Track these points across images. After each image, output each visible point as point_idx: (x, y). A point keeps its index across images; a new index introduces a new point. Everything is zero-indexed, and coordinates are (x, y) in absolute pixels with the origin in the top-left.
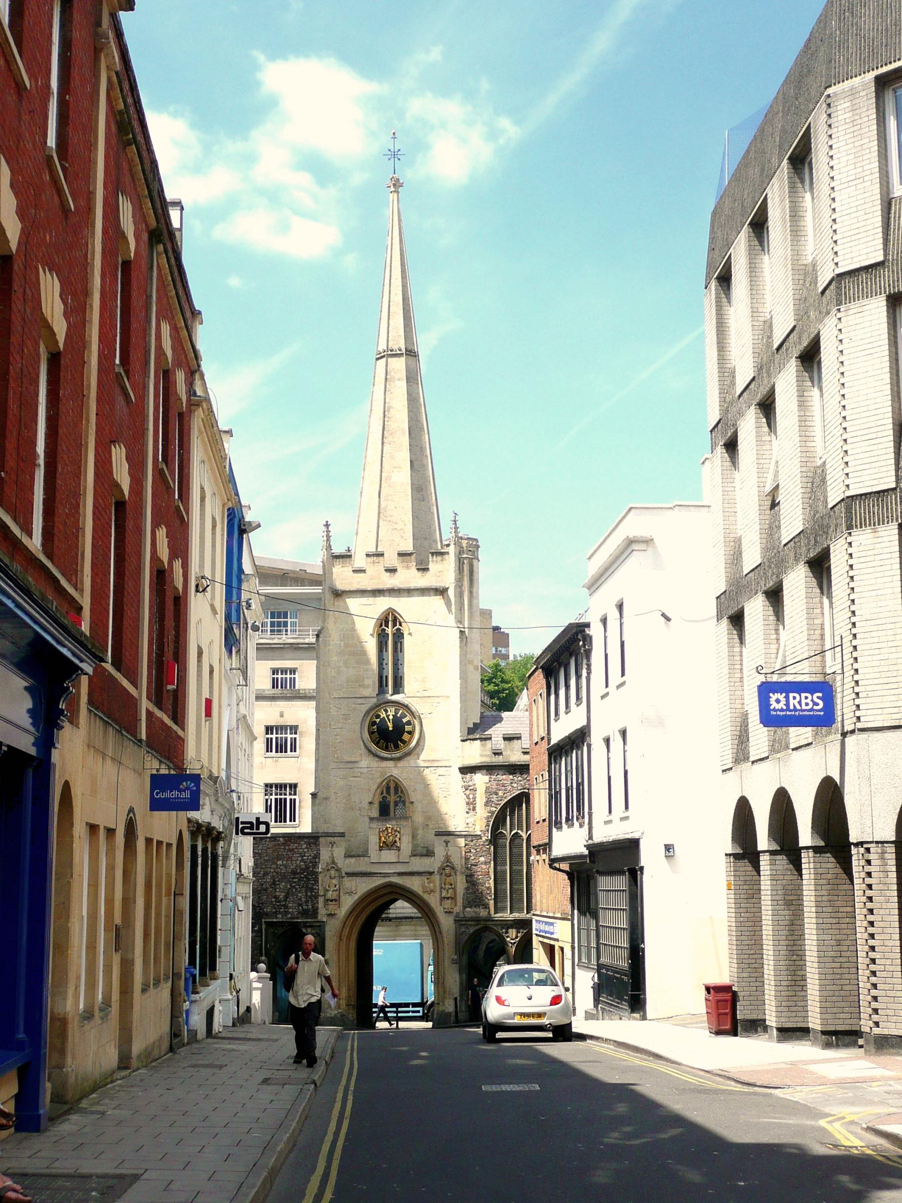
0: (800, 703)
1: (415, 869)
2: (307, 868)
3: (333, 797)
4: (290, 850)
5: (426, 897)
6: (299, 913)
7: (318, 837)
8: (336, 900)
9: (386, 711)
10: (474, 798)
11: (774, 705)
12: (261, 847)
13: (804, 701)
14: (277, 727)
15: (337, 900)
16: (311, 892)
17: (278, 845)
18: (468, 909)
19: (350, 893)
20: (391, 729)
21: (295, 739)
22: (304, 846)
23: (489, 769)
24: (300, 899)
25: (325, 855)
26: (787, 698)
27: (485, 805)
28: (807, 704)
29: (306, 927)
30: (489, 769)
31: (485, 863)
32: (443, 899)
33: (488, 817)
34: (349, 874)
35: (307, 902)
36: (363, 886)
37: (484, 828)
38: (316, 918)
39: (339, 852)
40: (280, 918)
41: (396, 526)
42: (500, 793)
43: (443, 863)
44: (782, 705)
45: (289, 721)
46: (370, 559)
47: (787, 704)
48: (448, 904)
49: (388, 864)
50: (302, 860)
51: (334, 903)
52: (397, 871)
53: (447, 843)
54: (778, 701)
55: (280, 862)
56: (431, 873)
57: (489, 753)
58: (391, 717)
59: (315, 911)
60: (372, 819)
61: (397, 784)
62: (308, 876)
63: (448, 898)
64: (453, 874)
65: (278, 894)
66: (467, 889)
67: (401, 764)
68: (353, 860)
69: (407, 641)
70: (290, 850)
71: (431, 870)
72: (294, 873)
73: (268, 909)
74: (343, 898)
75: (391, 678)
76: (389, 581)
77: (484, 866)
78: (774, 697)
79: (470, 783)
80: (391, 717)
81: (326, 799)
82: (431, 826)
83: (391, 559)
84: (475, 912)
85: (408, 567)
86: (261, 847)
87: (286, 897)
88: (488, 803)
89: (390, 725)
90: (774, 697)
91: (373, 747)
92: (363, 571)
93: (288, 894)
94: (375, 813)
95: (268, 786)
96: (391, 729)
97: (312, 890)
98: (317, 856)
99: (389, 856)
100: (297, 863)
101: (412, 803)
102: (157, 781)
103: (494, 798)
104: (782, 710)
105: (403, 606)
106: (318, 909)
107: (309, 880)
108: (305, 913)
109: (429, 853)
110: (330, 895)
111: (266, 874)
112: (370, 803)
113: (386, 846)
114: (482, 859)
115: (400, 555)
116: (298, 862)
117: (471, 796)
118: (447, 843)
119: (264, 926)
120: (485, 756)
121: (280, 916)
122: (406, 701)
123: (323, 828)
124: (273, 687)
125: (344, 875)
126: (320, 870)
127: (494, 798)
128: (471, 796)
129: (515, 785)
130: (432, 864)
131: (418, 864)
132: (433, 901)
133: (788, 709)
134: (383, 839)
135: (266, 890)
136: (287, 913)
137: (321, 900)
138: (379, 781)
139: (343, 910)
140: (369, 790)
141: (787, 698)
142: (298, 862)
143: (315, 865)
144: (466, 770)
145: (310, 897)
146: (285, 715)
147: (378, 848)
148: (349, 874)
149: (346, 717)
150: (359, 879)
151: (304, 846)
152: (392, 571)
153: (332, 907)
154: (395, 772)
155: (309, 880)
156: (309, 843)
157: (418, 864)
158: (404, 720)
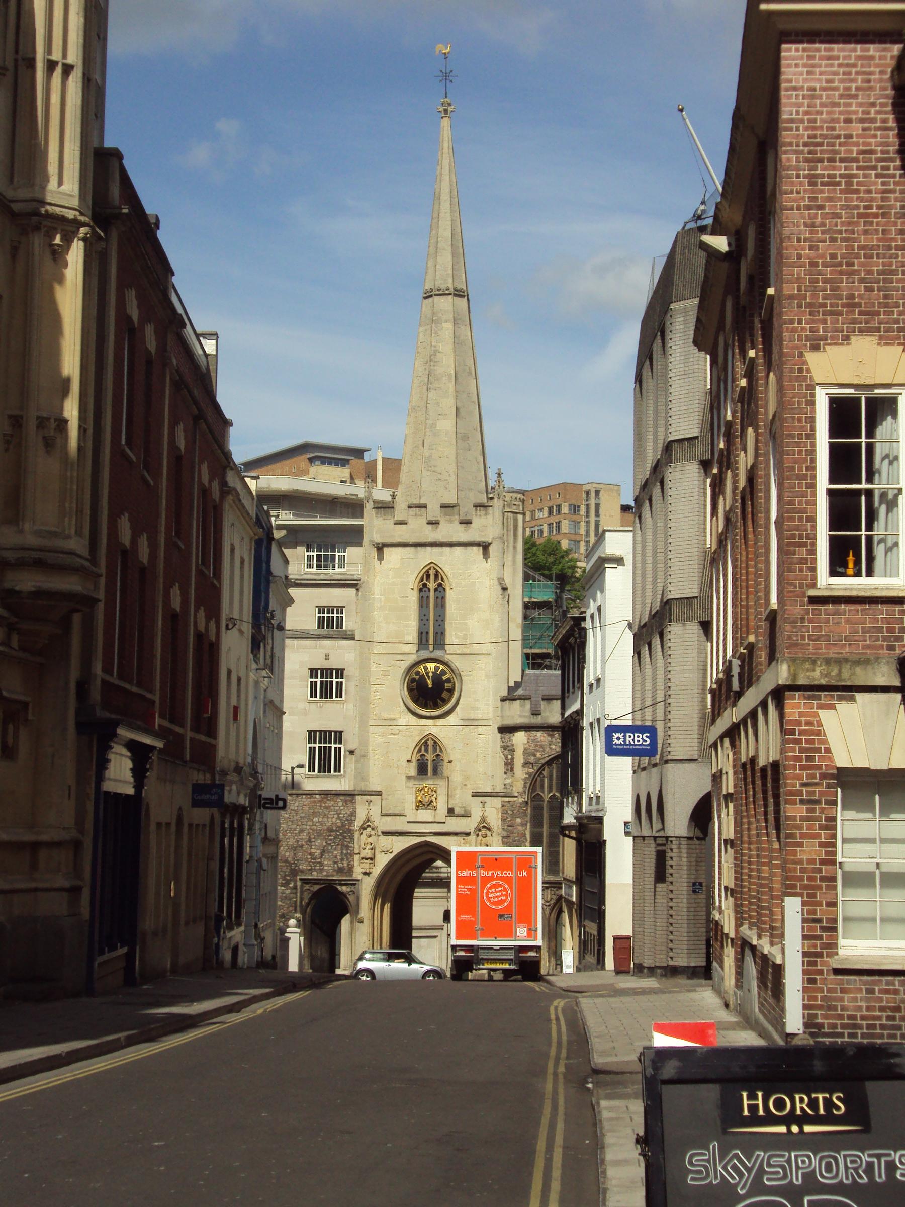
0: (633, 740)
1: (451, 830)
2: (343, 826)
3: (371, 753)
4: (326, 808)
6: (334, 870)
7: (355, 795)
8: (371, 859)
10: (513, 759)
11: (616, 741)
12: (297, 804)
13: (636, 739)
14: (322, 670)
16: (347, 850)
17: (315, 802)
19: (386, 852)
20: (430, 686)
21: (341, 683)
22: (340, 804)
23: (527, 728)
24: (336, 857)
26: (625, 736)
28: (638, 741)
29: (342, 885)
30: (527, 728)
31: (522, 825)
33: (526, 779)
34: (385, 833)
35: (342, 860)
36: (400, 845)
37: (521, 790)
38: (351, 875)
39: (375, 811)
40: (315, 875)
41: (439, 476)
42: (538, 755)
43: (480, 823)
44: (621, 741)
45: (334, 664)
46: (413, 511)
47: (625, 741)
49: (425, 824)
50: (339, 818)
51: (368, 861)
52: (433, 831)
53: (483, 803)
54: (618, 739)
55: (315, 820)
56: (468, 834)
57: (528, 713)
58: (431, 675)
59: (350, 870)
60: (409, 778)
61: (435, 742)
62: (343, 834)
65: (313, 851)
67: (440, 722)
69: (450, 596)
70: (326, 808)
71: (468, 831)
72: (330, 830)
73: (303, 866)
75: (432, 633)
76: (431, 535)
77: (520, 828)
78: (616, 736)
79: (509, 744)
80: (431, 675)
81: (364, 756)
82: (469, 786)
83: (434, 511)
85: (451, 521)
86: (297, 804)
87: (322, 855)
89: (430, 683)
90: (616, 736)
91: (413, 706)
92: (403, 523)
93: (323, 851)
94: (413, 771)
95: (312, 734)
96: (430, 686)
97: (347, 847)
98: (353, 814)
99: (425, 815)
100: (332, 820)
101: (450, 762)
102: (198, 788)
104: (621, 744)
105: (446, 560)
107: (344, 837)
108: (340, 870)
109: (466, 815)
110: (367, 853)
111: (302, 831)
112: (408, 761)
113: (421, 805)
114: (519, 820)
115: (443, 506)
116: (334, 820)
117: (510, 757)
118: (483, 803)
119: (299, 883)
120: (524, 716)
121: (314, 873)
122: (447, 658)
123: (362, 786)
124: (319, 627)
125: (380, 833)
128: (510, 757)
129: (553, 747)
130: (469, 825)
131: (454, 824)
133: (625, 744)
135: (302, 846)
136: (321, 870)
137: (356, 858)
139: (377, 870)
141: (625, 736)
142: (334, 820)
143: (351, 822)
144: (506, 730)
145: (346, 855)
146: (331, 658)
147: (414, 807)
148: (385, 833)
149: (386, 674)
151: (340, 804)
152: (434, 523)
154: (434, 731)
155: (344, 837)
156: (346, 801)
157: (454, 824)
158: (444, 678)
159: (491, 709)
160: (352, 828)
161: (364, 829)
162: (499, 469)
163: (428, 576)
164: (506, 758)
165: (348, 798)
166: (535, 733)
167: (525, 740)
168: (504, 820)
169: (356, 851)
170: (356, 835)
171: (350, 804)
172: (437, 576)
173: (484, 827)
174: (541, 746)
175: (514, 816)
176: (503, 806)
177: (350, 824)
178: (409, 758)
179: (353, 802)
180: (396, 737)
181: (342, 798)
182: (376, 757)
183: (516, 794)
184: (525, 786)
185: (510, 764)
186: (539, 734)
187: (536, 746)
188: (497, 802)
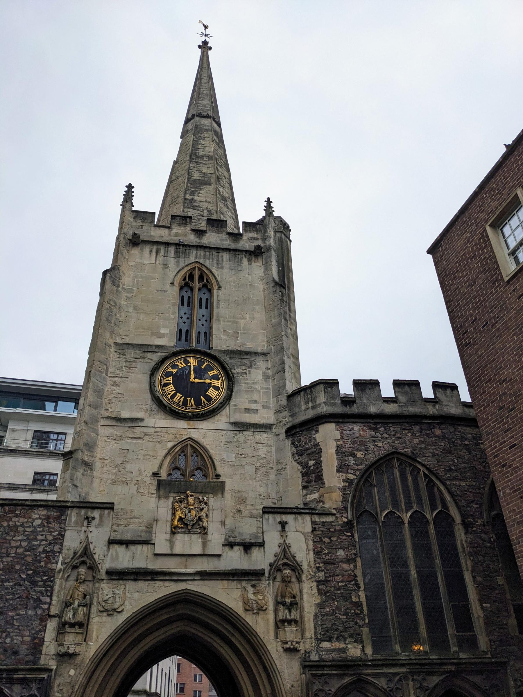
3: (98, 464)
5: (249, 619)
8: (80, 625)
9: (187, 362)
10: (318, 464)
18: (326, 645)
19: (111, 612)
22: (39, 522)
27: (338, 471)
32: (280, 624)
36: (138, 597)
37: (340, 505)
41: (201, 213)
42: (359, 454)
48: (290, 633)
51: (77, 629)
63: (290, 622)
64: (294, 579)
66: (320, 606)
68: (121, 550)
74: (95, 620)
77: (345, 566)
84: (344, 651)
88: (340, 469)
98: (59, 540)
103: (351, 461)
113: (184, 526)
114: (341, 553)
117: (311, 463)
118: (283, 524)
127: (351, 461)
128: (311, 463)
129: (380, 444)
130: (261, 560)
131: (234, 559)
132: (263, 626)
134: (179, 514)
137: (52, 625)
138: (170, 445)
140: (155, 457)
143: (51, 555)
147: (169, 530)
150: (131, 585)
153: (71, 639)
154: (195, 435)
155: (34, 583)
159: (272, 411)
160: (54, 566)
161: (75, 567)
162: (269, 199)
163: (191, 277)
164: (305, 466)
165: (54, 513)
166: (350, 426)
167: (337, 435)
168: (317, 553)
169: (54, 611)
171: (54, 525)
172: (201, 278)
173: (285, 564)
174: (362, 443)
175: (332, 546)
176: (314, 530)
178: (155, 470)
180: (139, 441)
181: (44, 512)
182: (105, 469)
183: (334, 512)
184: (345, 500)
185: (313, 472)
186: (356, 428)
187: (354, 443)
188: (305, 524)
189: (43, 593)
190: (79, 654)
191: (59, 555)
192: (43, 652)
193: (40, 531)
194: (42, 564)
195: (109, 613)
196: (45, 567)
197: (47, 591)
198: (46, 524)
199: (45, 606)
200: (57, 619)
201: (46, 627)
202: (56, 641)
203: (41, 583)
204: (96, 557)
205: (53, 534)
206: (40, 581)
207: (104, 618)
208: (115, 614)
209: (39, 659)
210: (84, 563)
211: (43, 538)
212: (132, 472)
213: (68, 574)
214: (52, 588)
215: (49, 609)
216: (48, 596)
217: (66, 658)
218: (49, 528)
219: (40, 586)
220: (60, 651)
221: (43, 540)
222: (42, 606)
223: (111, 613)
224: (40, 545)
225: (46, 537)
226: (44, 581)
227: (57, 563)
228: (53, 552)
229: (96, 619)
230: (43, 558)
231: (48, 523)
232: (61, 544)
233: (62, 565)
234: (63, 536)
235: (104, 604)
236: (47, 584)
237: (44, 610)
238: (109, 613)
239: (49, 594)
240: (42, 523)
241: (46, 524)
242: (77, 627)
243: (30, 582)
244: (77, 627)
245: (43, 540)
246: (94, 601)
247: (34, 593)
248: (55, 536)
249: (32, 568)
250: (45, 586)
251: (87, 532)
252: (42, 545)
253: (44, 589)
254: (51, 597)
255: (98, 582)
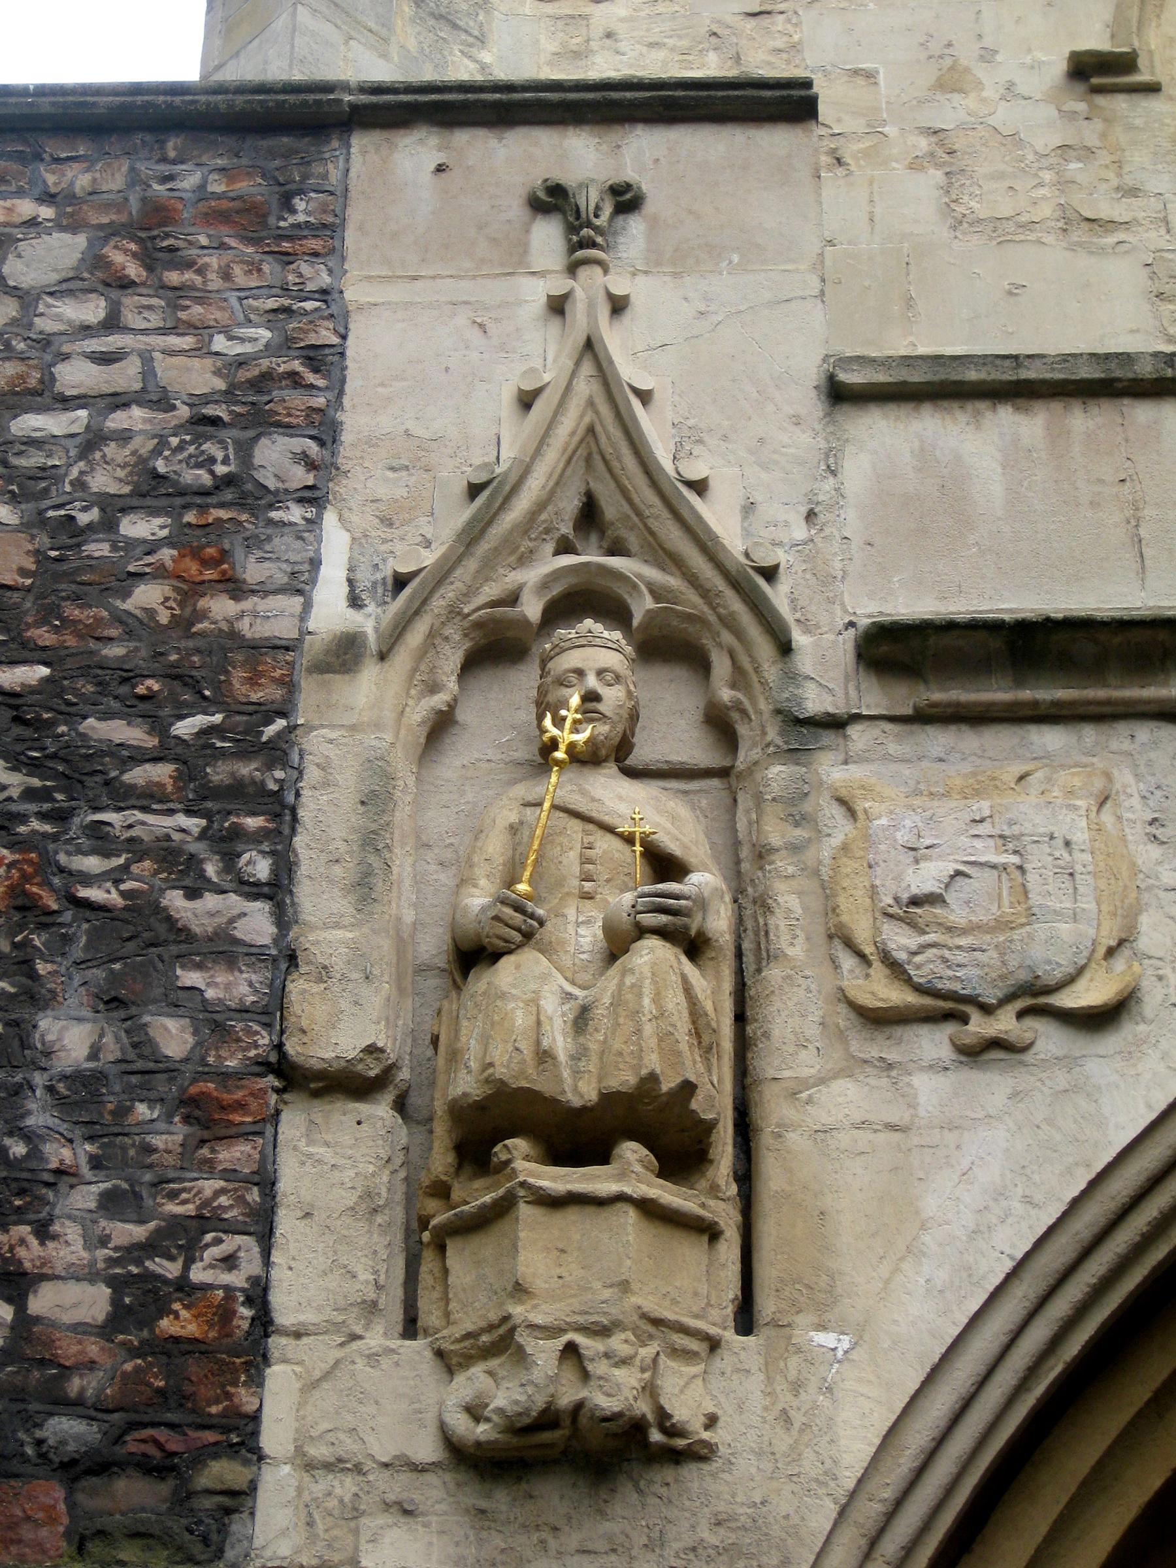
15: (678, 1137)
19: (995, 1017)
25: (445, 344)
34: (971, 670)
74: (836, 1114)
98: (293, 384)
106: (247, 1336)
107: (81, 777)
125: (824, 674)
126: (330, 611)
137: (334, 1175)
148: (971, 670)
153: (583, 1269)
160: (271, 618)
161: (496, 647)
165: (197, 177)
170: (347, 734)
171: (220, 263)
177: (209, 563)
179: (290, 234)
189: (194, 862)
190: (700, 1454)
191: (314, 523)
192: (274, 1437)
193: (86, 330)
194: (148, 596)
195: (979, 1027)
196: (183, 624)
197: (228, 844)
198: (133, 270)
199: (235, 986)
200: (381, 1110)
201: (266, 1181)
202: (411, 1327)
203: (162, 772)
204: (719, 516)
205: (220, 343)
206: (139, 757)
207: (929, 1090)
208: (1050, 1039)
209: (238, 1500)
210: (578, 601)
211: (126, 376)
212: (870, 76)
213: (439, 700)
214: (282, 811)
215: (273, 1009)
216: (252, 890)
217: (554, 1495)
218: (177, 295)
219: (149, 799)
220: (475, 1412)
221: (118, 401)
222: (191, 978)
223: (1005, 1024)
224: (91, 443)
225: (148, 372)
226: (189, 758)
227: (300, 584)
228: (244, 491)
229: (846, 1100)
230: (151, 547)
231: (154, 257)
232: (325, 429)
233: (355, 602)
234: (324, 360)
235: (900, 940)
236: (219, 773)
237: (214, 1023)
238: (979, 1027)
239: (262, 869)
240: (96, 262)
241: (133, 270)
242: (631, 1152)
243: (34, 767)
244: (631, 1152)
245: (118, 401)
246: (778, 922)
247: (92, 864)
248: (241, 362)
249: (44, 636)
250: (198, 795)
251: (578, 310)
252: (124, 437)
253: (194, 824)
254: (276, 891)
255: (794, 754)
